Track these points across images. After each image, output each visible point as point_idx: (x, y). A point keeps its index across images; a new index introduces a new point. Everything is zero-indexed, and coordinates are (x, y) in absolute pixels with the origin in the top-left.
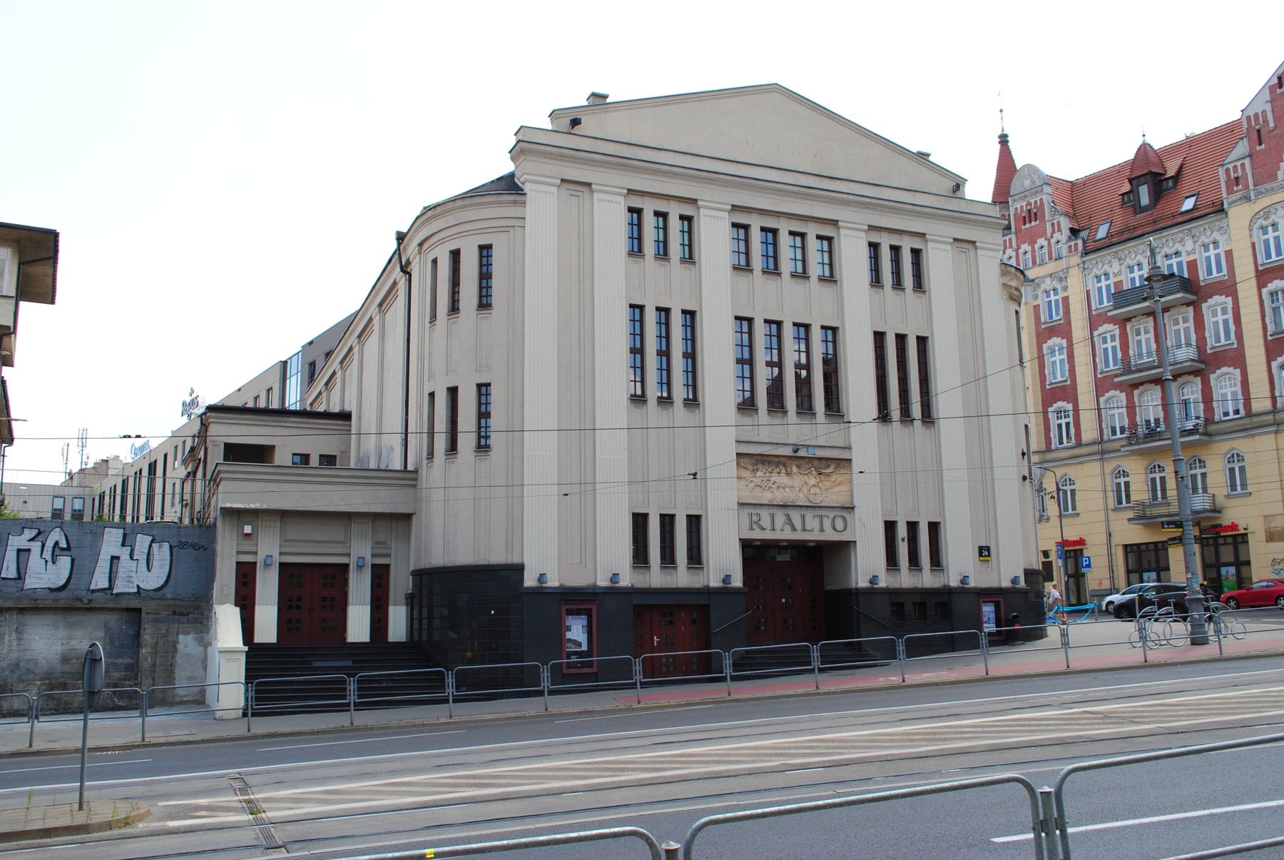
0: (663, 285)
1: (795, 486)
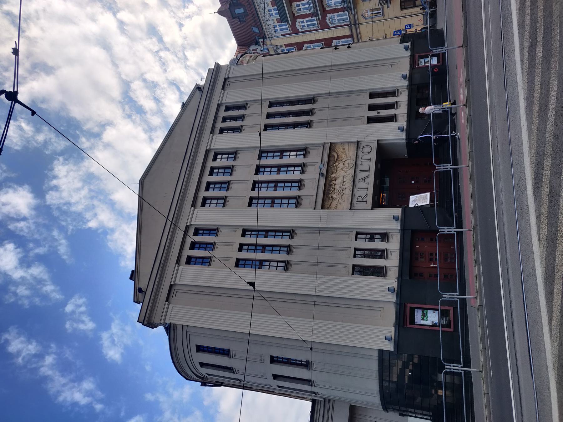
0: (227, 247)
1: (343, 176)
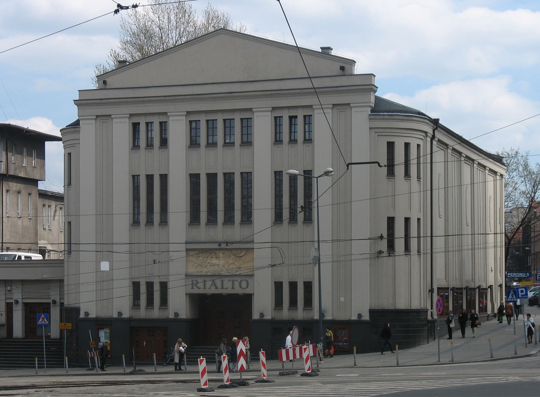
0: (149, 162)
1: (220, 264)
